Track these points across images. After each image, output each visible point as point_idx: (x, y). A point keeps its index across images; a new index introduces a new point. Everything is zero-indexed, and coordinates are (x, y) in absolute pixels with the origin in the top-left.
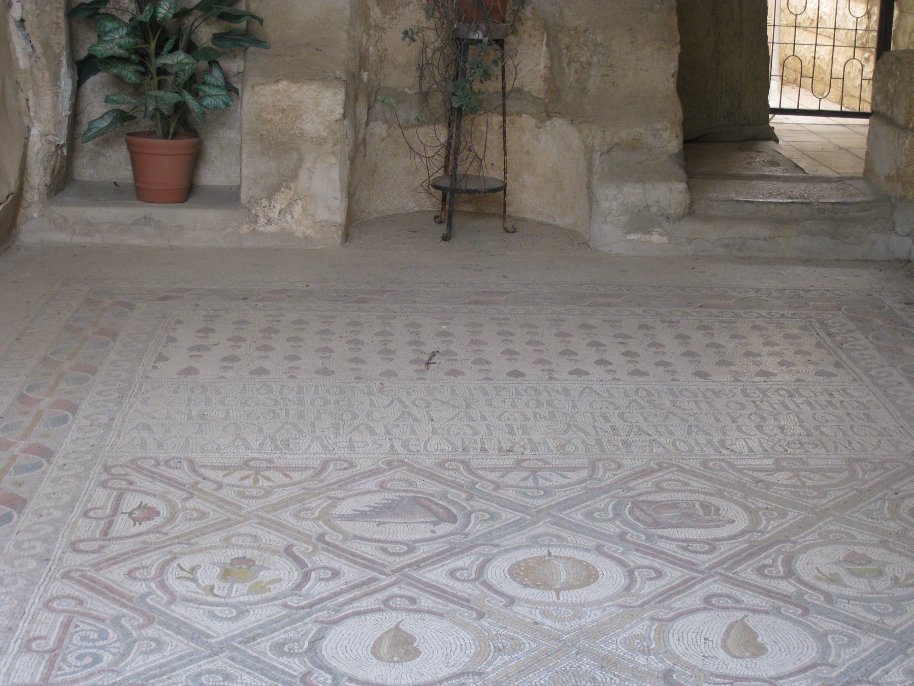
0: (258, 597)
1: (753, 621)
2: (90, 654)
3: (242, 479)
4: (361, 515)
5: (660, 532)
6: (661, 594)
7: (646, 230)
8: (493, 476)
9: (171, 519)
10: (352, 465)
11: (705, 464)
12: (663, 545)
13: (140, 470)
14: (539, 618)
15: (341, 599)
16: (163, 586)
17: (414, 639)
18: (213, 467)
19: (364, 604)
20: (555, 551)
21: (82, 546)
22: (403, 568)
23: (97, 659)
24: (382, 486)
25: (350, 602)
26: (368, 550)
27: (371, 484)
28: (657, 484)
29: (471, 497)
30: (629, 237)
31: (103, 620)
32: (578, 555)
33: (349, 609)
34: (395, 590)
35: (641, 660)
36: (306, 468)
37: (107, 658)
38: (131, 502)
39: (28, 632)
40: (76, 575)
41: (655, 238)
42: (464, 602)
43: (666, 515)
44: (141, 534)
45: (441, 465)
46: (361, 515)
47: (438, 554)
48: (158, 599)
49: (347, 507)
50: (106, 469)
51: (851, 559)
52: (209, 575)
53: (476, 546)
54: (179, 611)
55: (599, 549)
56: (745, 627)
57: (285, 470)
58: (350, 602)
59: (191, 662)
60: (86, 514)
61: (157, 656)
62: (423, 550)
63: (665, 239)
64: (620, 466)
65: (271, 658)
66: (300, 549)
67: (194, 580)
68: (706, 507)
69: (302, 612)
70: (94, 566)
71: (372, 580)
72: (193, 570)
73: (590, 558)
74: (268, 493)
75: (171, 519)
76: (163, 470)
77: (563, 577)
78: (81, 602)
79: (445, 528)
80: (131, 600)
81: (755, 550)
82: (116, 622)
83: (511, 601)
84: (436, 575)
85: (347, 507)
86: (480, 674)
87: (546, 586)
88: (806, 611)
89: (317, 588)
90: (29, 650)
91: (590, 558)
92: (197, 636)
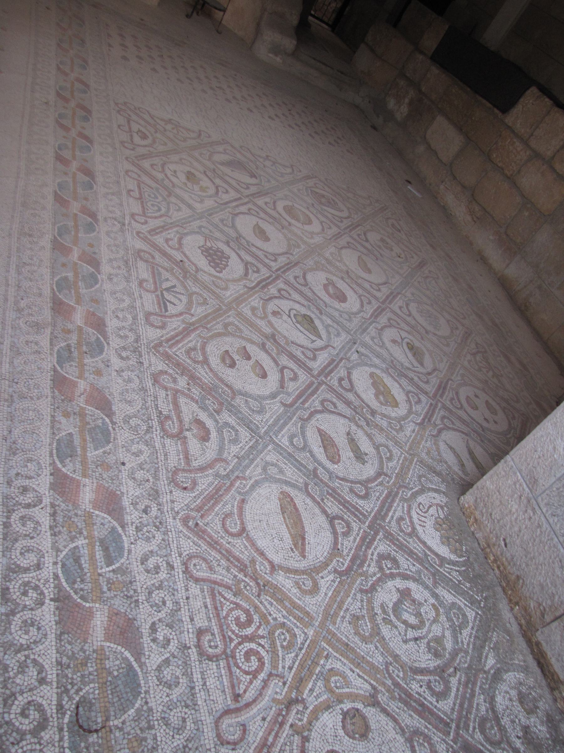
0: (204, 194)
1: (364, 257)
2: (158, 206)
3: (173, 129)
4: (222, 164)
5: (324, 207)
6: (333, 236)
7: (276, 54)
8: (261, 160)
9: (154, 141)
10: (209, 137)
11: (326, 179)
12: (326, 213)
13: (130, 109)
14: (301, 235)
15: (234, 204)
16: (166, 175)
17: (265, 233)
18: (162, 120)
19: (243, 209)
20: (295, 205)
21: (126, 144)
22: (247, 196)
23: (160, 210)
24: (225, 152)
25: (237, 206)
26: (234, 183)
27: (220, 148)
28: (315, 184)
29: (257, 168)
30: (271, 55)
31: (152, 188)
32: (303, 210)
33: (237, 211)
34: (250, 206)
35: (338, 264)
36: (193, 132)
37: (163, 210)
38: (135, 127)
39: (126, 186)
40: (131, 160)
41: (278, 59)
42: (275, 219)
43: (323, 200)
44: (146, 146)
45: (241, 147)
46: (222, 164)
47: (257, 193)
48: (166, 182)
49: (216, 157)
50: (116, 104)
51: (382, 240)
52: (183, 178)
53: (268, 193)
54: (178, 191)
55: (308, 208)
56: (363, 260)
57: (188, 130)
58: (237, 206)
59: (195, 220)
60: (119, 126)
61: (180, 213)
62: (253, 189)
63: (281, 61)
64: (300, 171)
65: (221, 225)
66: (209, 174)
67: (177, 177)
68: (334, 201)
69: (223, 207)
70: (136, 157)
71: (240, 199)
72: (175, 172)
73: (307, 212)
74: (185, 140)
75: (154, 141)
76: (138, 112)
77: (302, 217)
78: (139, 176)
79: (253, 181)
80: (158, 180)
81: (353, 227)
82: (157, 189)
83: (290, 224)
84: (260, 202)
85: (216, 157)
86: (292, 254)
87: (298, 220)
88: (377, 259)
89: (225, 197)
90: (131, 196)
91: (307, 212)
92: (190, 206)
